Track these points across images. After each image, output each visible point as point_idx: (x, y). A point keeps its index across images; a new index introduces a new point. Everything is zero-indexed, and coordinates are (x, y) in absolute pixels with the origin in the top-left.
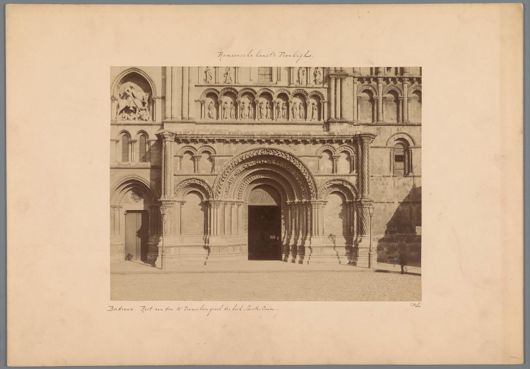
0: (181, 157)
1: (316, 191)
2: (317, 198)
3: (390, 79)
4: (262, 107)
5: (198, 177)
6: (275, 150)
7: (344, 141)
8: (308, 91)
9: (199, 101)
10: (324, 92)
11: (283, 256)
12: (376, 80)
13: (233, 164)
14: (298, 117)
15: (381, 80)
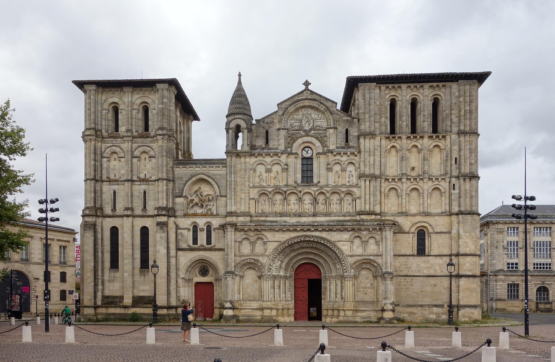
3: (412, 179)
9: (253, 199)
11: (323, 318)
15: (404, 180)
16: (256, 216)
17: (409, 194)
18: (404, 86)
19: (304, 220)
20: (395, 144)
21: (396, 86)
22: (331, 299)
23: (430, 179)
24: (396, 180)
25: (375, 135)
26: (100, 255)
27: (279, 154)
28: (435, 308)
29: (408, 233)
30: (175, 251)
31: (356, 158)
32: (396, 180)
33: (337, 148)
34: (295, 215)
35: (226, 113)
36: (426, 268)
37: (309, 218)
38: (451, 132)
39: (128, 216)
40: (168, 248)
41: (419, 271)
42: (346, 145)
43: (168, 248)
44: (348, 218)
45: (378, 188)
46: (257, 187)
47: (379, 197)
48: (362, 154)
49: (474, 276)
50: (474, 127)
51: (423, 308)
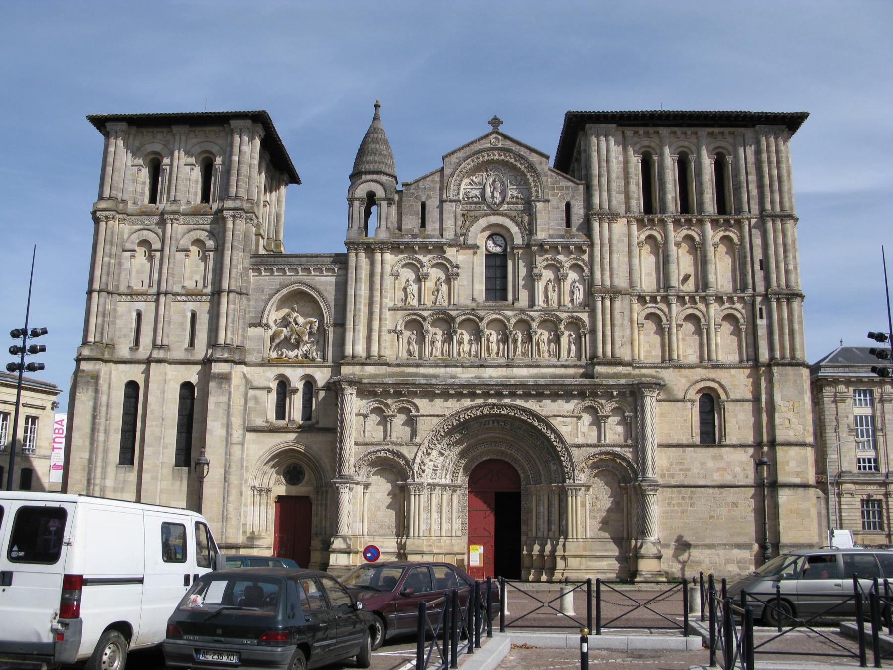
0: (365, 416)
1: (573, 471)
2: (574, 480)
3: (687, 298)
4: (491, 340)
5: (391, 447)
6: (510, 407)
7: (615, 393)
8: (563, 315)
9: (395, 331)
10: (585, 316)
11: (523, 573)
12: (665, 299)
13: (446, 428)
14: (546, 355)
15: (673, 300)
16: (398, 365)
17: (681, 325)
18: (664, 131)
19: (489, 374)
20: (655, 233)
21: (651, 130)
22: (540, 534)
23: (719, 299)
24: (659, 298)
25: (617, 215)
26: (101, 437)
27: (445, 247)
28: (736, 551)
29: (683, 400)
30: (240, 432)
31: (586, 257)
32: (659, 298)
33: (551, 236)
34: (472, 366)
35: (350, 171)
36: (718, 470)
37: (499, 369)
38: (749, 212)
39: (159, 361)
40: (228, 426)
41: (705, 477)
42: (566, 232)
43: (228, 426)
44: (571, 371)
45: (627, 313)
46: (402, 309)
47: (628, 331)
48: (597, 248)
49: (805, 486)
50: (787, 205)
51: (714, 551)
